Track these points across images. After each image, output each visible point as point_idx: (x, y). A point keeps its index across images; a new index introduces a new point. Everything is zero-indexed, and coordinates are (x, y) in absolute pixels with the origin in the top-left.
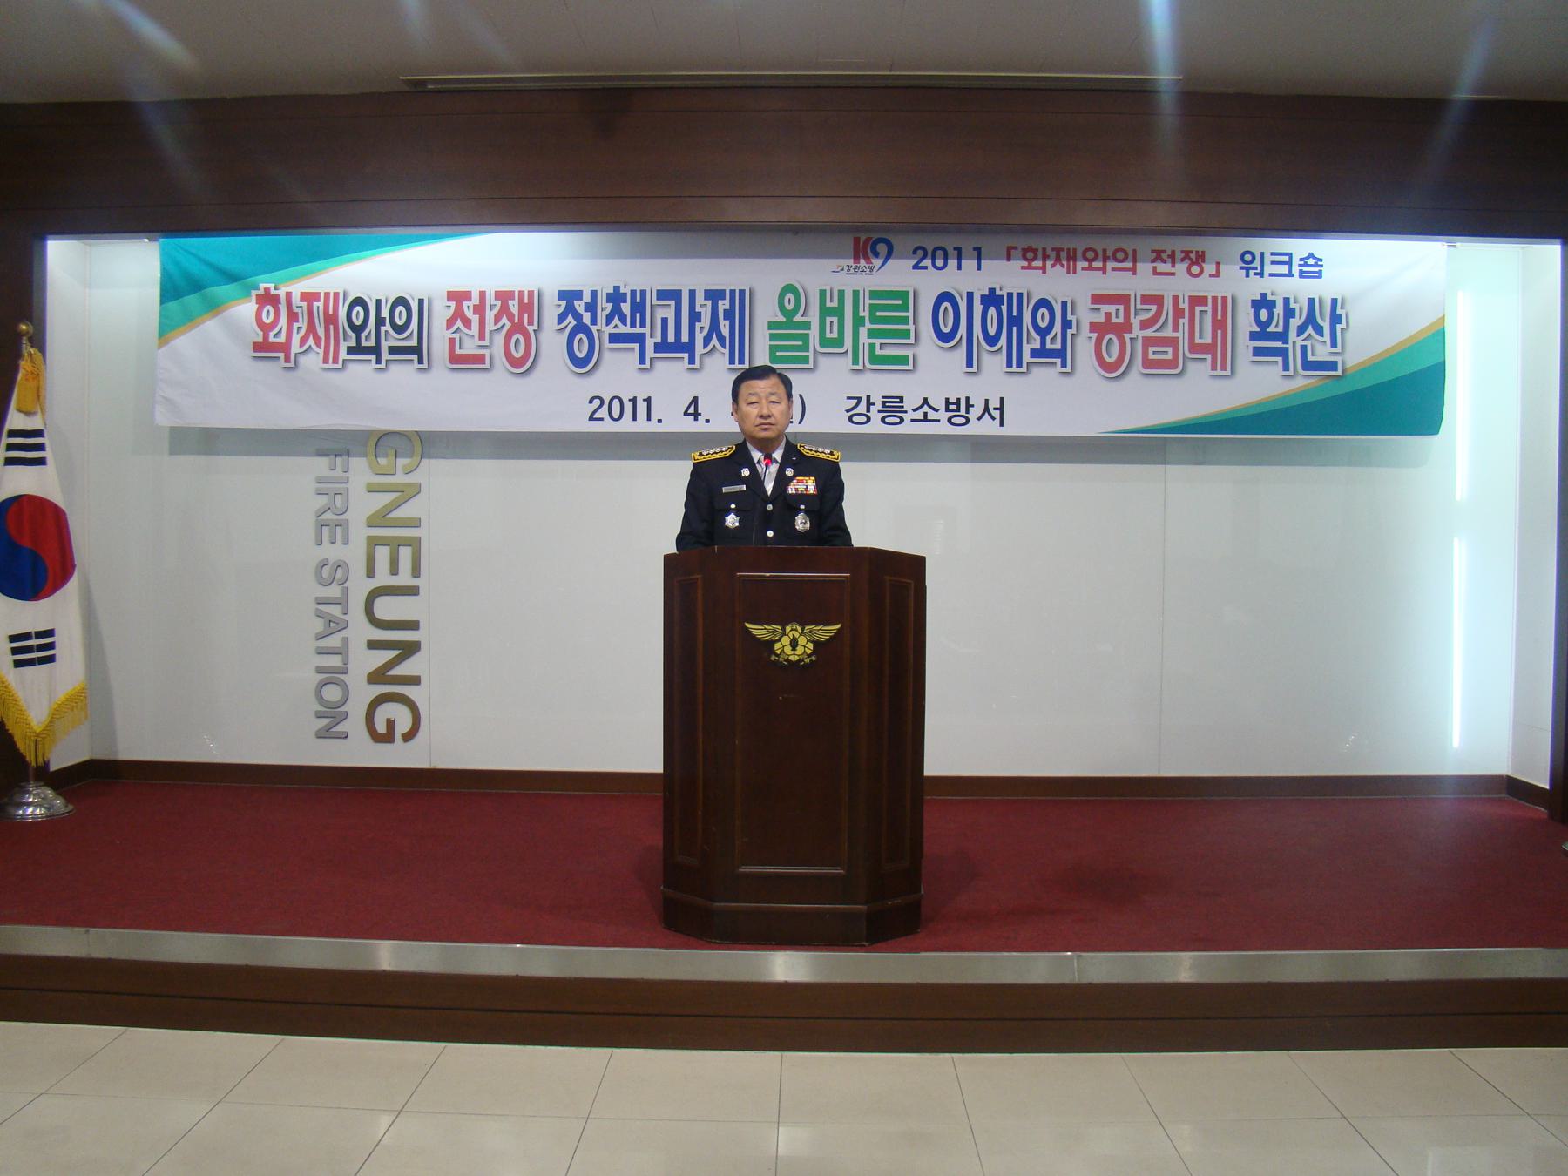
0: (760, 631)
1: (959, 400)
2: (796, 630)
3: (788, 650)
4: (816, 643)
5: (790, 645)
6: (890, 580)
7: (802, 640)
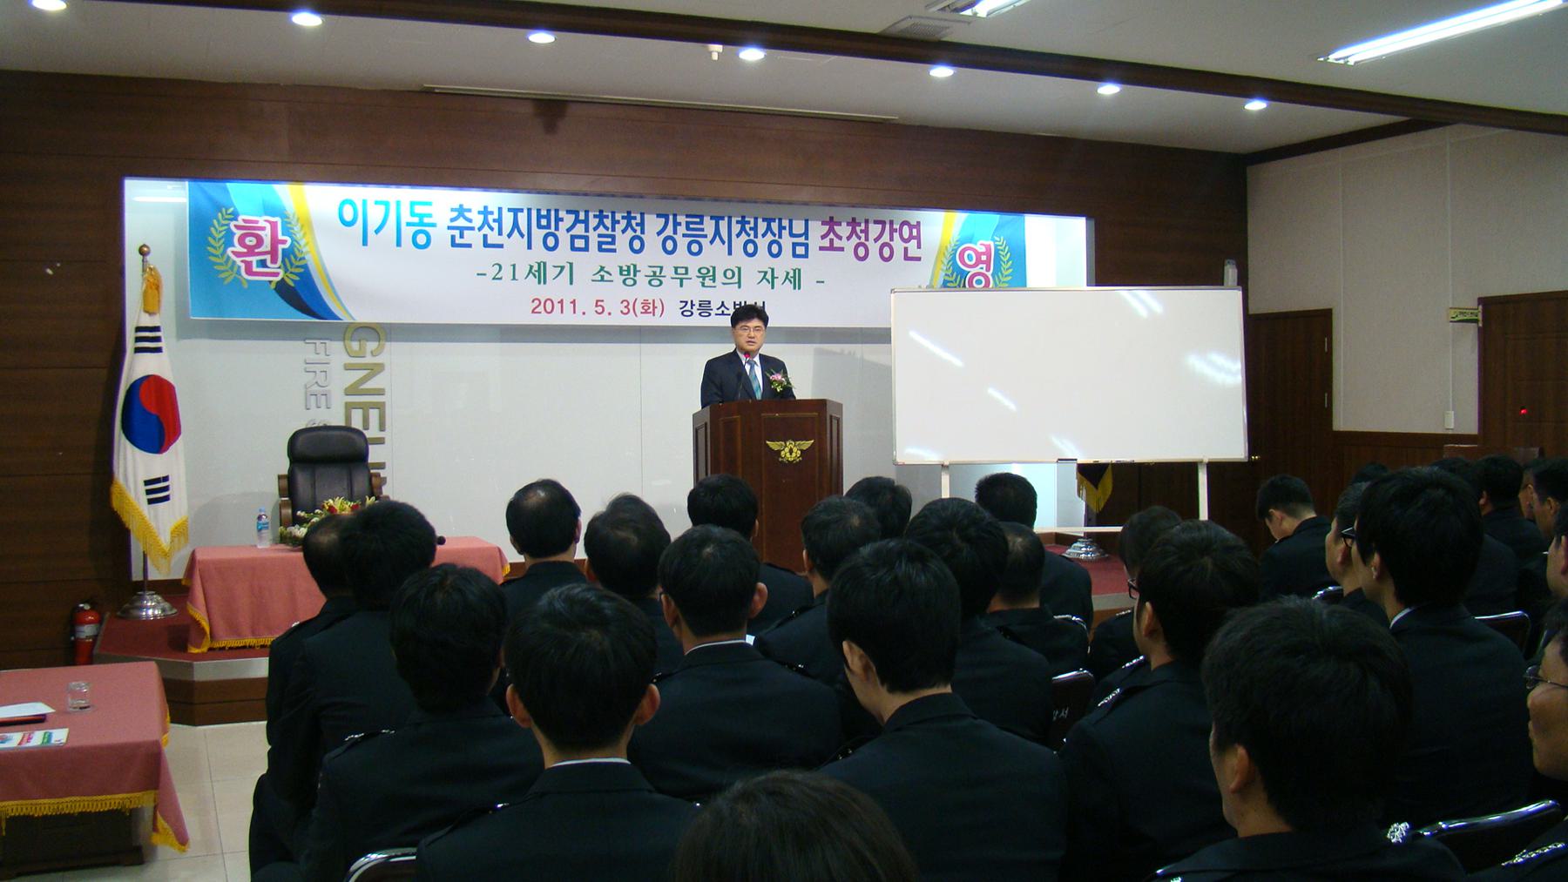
0: (774, 445)
3: (788, 455)
4: (802, 451)
7: (795, 450)
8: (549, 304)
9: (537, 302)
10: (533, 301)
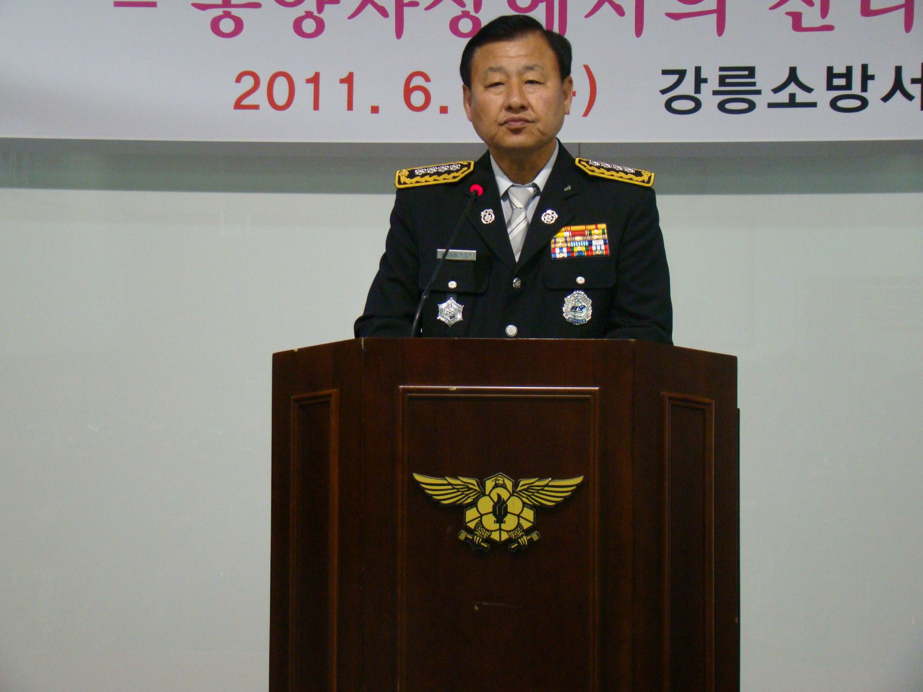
1: (849, 69)
2: (504, 486)
3: (489, 522)
4: (539, 510)
5: (494, 512)
6: (670, 399)
7: (514, 505)
8: (281, 85)
9: (248, 82)
10: (238, 80)
